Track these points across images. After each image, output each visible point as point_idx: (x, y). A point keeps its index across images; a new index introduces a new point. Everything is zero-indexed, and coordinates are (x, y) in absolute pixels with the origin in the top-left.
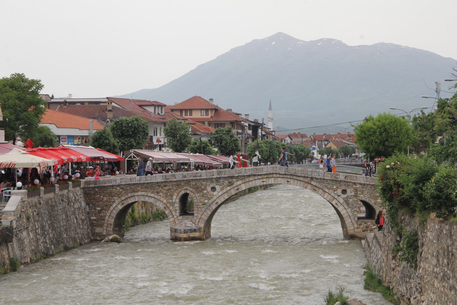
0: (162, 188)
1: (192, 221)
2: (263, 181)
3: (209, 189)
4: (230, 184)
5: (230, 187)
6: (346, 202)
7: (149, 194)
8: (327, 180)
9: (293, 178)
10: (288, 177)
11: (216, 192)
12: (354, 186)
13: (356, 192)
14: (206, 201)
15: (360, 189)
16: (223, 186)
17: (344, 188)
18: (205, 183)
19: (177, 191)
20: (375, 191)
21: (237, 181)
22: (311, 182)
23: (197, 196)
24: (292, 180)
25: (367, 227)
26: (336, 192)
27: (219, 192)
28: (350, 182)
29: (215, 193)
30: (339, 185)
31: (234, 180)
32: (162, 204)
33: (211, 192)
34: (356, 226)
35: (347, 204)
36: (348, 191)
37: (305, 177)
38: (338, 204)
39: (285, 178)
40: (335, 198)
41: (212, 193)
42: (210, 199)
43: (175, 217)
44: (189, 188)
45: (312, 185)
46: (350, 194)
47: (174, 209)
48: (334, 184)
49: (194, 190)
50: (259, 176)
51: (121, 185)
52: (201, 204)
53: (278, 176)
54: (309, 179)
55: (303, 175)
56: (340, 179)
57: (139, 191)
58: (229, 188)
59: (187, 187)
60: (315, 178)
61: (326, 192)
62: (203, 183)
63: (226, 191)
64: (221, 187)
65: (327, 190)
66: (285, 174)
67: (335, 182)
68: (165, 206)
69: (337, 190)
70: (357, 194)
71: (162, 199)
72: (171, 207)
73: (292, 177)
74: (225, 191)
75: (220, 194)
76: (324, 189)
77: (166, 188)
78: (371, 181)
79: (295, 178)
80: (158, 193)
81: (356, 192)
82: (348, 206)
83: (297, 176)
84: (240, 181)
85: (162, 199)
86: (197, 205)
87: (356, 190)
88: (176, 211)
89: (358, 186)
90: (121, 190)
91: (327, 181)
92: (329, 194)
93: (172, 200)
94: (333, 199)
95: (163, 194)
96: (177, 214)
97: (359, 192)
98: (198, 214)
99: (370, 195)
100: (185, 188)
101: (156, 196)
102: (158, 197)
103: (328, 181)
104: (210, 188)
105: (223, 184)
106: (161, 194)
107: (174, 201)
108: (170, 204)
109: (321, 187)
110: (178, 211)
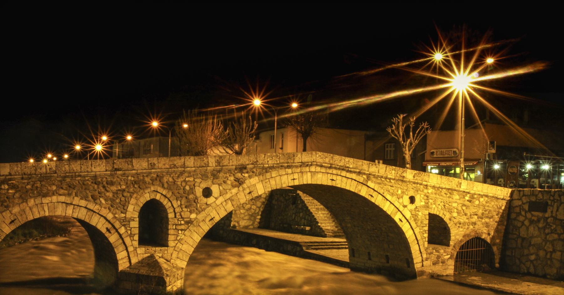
0: (104, 187)
1: (165, 256)
2: (294, 179)
3: (199, 191)
4: (237, 183)
5: (236, 189)
6: (413, 217)
7: (76, 201)
8: (390, 179)
9: (342, 175)
10: (335, 172)
11: (212, 197)
12: (425, 191)
13: (427, 201)
14: (193, 216)
15: (432, 195)
16: (225, 186)
17: (411, 193)
18: (192, 179)
19: (135, 195)
20: (451, 199)
21: (250, 177)
22: (367, 181)
23: (175, 206)
24: (339, 178)
25: (438, 257)
26: (401, 200)
27: (216, 198)
28: (421, 184)
29: (211, 200)
30: (405, 188)
31: (246, 175)
32: (103, 220)
33: (202, 198)
34: (425, 256)
35: (415, 220)
36: (417, 198)
37: (359, 173)
38: (403, 219)
39: (328, 173)
40: (399, 210)
41: (205, 200)
42: (200, 212)
43: (131, 249)
44: (160, 189)
45: (368, 187)
46: (419, 204)
47: (129, 232)
48: (399, 186)
49: (171, 193)
50: (287, 170)
51: (10, 180)
52: (183, 222)
53: (318, 169)
54: (365, 176)
55: (358, 170)
56: (408, 180)
57: (53, 194)
58: (235, 191)
59: (156, 187)
60: (374, 175)
61: (387, 200)
62: (187, 179)
63: (231, 195)
64: (221, 188)
65: (388, 197)
66: (330, 168)
67: (400, 183)
68: (110, 226)
69: (402, 197)
70: (428, 203)
71: (104, 212)
72: (123, 228)
73: (339, 172)
74: (228, 196)
75: (218, 202)
76: (384, 195)
77: (114, 188)
78: (446, 183)
79: (344, 173)
80: (94, 198)
81: (427, 201)
82: (416, 223)
83: (348, 171)
84: (257, 178)
85: (104, 212)
86: (176, 225)
87: (427, 197)
88: (131, 236)
89: (430, 191)
90: (10, 191)
91: (390, 182)
92: (391, 203)
93: (125, 213)
94: (397, 213)
95: (106, 200)
96: (134, 242)
97: (430, 201)
98: (176, 242)
99: (444, 206)
100: (152, 189)
101: (91, 206)
102: (96, 208)
103: (392, 181)
104: (201, 190)
105: (225, 182)
106: (103, 201)
107: (129, 215)
108: (121, 223)
109: (381, 192)
110: (136, 237)
